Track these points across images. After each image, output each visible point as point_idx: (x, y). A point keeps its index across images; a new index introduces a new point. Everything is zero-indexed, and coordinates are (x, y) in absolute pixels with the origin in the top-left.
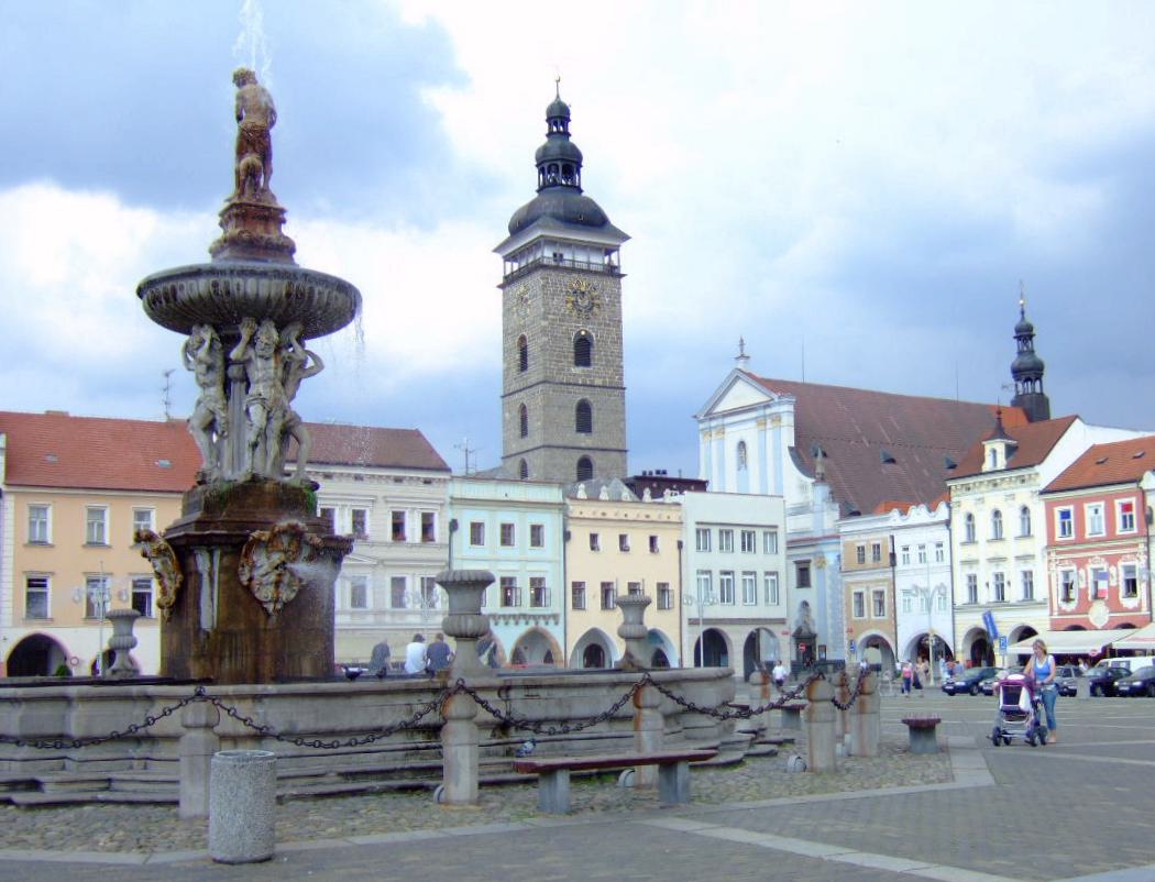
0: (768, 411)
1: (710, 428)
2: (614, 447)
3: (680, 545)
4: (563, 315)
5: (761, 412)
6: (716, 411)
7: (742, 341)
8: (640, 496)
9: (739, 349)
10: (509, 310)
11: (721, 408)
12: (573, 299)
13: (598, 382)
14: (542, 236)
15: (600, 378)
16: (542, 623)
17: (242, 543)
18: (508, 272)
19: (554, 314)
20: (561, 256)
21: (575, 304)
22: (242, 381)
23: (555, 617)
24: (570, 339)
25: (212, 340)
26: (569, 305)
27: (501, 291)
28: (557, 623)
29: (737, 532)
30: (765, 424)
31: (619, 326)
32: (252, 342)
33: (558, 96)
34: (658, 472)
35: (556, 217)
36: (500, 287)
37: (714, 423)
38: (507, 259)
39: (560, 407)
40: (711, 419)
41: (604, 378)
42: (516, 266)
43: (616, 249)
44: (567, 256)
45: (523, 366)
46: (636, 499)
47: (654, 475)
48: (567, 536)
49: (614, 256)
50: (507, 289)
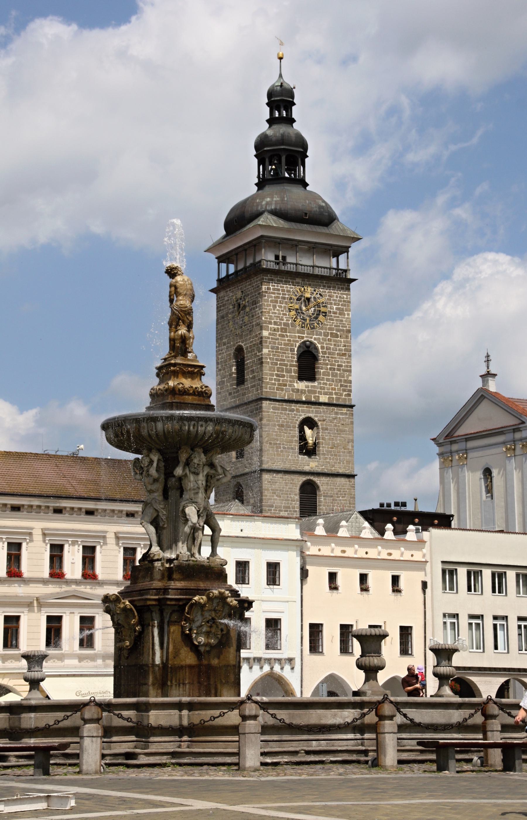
0: (518, 435)
1: (451, 452)
2: (341, 471)
3: (424, 585)
4: (285, 324)
5: (509, 437)
6: (457, 434)
7: (488, 356)
8: (382, 532)
9: (485, 364)
10: (223, 317)
11: (462, 431)
12: (297, 306)
13: (324, 399)
14: (262, 237)
15: (325, 394)
16: (277, 668)
17: (185, 605)
18: (223, 274)
19: (275, 323)
20: (284, 258)
21: (299, 311)
22: (177, 489)
23: (290, 660)
24: (292, 350)
25: (159, 460)
26: (293, 313)
27: (214, 296)
28: (292, 668)
29: (487, 573)
30: (514, 449)
31: (347, 337)
32: (187, 464)
33: (281, 76)
34: (397, 504)
35: (275, 213)
36: (212, 291)
37: (455, 447)
38: (221, 259)
39: (282, 426)
40: (452, 443)
41: (331, 394)
42: (232, 269)
43: (345, 250)
44: (290, 259)
45: (241, 380)
46: (377, 535)
47: (393, 507)
48: (304, 574)
49: (342, 258)
50: (222, 294)
